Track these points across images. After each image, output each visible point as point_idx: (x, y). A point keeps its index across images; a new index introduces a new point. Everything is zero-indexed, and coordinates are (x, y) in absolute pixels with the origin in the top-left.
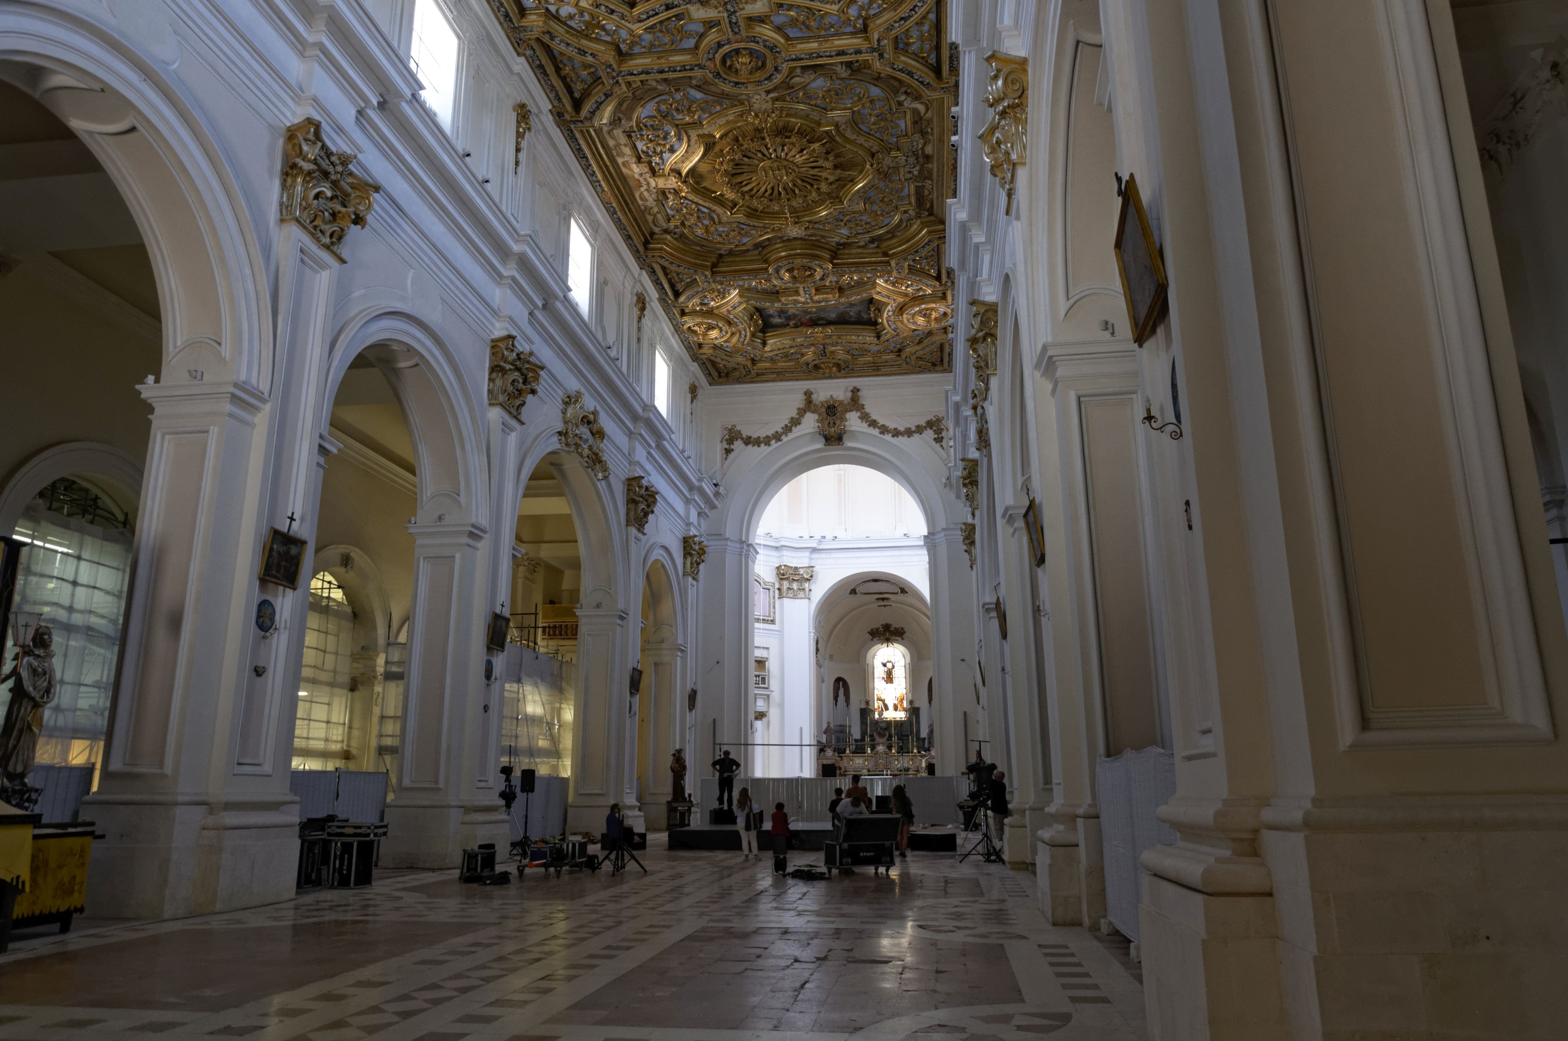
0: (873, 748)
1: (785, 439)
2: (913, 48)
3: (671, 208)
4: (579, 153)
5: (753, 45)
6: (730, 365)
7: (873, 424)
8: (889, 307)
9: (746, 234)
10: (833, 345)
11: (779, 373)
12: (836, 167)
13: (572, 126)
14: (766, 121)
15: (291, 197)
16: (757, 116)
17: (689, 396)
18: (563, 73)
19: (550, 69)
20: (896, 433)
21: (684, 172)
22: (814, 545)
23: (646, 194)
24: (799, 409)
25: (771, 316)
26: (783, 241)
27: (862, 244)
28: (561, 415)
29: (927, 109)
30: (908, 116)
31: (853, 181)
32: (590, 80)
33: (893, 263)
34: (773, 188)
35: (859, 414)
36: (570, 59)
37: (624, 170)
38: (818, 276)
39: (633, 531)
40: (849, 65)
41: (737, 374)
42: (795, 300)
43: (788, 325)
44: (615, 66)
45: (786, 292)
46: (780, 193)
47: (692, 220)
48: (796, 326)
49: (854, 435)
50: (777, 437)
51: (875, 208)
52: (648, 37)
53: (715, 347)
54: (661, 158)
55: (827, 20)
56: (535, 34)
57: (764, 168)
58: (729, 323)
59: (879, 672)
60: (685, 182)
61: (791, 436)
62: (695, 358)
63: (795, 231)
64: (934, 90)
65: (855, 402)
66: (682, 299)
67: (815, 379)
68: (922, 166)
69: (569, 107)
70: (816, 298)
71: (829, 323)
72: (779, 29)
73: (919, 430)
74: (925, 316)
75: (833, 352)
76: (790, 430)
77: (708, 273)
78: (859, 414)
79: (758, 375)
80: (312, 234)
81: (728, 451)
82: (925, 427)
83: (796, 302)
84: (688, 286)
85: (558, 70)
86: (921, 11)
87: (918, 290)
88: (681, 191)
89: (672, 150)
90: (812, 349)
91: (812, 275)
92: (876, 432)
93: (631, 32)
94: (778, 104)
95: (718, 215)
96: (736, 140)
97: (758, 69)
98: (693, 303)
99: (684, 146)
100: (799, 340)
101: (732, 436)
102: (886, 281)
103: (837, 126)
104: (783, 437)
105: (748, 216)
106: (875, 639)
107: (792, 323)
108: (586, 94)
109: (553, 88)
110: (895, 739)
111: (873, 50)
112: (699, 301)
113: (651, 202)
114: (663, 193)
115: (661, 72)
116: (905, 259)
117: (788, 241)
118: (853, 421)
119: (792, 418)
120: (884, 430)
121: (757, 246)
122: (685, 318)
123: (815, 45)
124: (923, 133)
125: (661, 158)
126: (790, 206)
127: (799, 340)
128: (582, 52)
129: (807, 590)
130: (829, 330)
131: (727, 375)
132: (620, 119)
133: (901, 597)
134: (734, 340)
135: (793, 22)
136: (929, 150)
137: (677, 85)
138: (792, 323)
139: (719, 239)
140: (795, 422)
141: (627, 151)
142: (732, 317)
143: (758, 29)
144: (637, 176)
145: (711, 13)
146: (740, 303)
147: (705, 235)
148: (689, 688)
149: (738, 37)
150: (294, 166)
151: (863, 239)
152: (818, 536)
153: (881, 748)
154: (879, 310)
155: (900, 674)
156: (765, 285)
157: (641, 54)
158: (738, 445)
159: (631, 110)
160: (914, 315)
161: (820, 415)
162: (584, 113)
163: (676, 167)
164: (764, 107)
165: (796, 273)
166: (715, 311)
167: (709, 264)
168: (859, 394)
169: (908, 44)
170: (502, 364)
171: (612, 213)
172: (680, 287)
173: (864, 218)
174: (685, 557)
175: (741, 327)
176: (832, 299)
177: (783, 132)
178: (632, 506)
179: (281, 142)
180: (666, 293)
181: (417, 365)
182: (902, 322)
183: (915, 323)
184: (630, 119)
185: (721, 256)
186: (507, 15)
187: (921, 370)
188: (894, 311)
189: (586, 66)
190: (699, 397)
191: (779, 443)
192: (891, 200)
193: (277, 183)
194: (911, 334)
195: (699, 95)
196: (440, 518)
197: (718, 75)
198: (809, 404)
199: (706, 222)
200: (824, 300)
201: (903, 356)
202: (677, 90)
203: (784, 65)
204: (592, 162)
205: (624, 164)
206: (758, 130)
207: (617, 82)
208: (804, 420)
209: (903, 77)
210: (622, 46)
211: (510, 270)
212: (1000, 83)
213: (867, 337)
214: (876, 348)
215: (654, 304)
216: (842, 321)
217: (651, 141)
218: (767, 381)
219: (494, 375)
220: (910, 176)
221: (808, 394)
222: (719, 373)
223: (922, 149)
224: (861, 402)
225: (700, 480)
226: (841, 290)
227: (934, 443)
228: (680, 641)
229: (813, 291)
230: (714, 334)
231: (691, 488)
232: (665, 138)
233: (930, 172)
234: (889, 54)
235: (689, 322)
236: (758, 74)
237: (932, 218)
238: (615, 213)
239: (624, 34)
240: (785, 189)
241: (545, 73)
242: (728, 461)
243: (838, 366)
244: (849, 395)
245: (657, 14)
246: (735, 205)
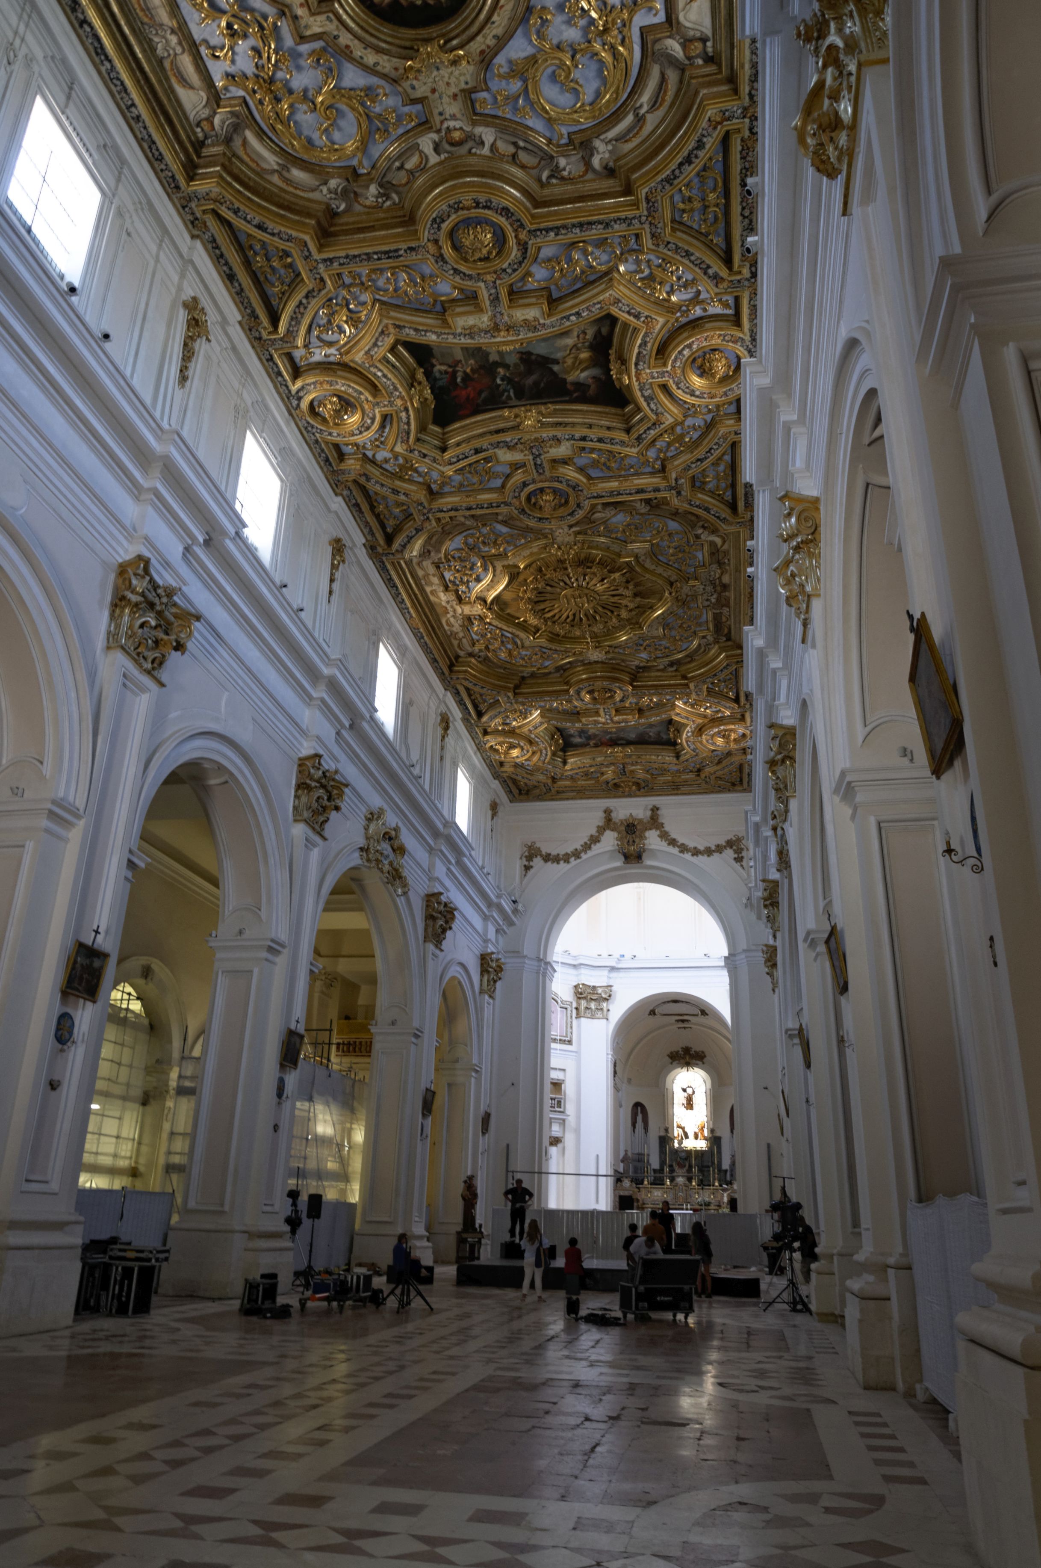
0: (672, 1180)
2: (710, 486)
3: (476, 633)
4: (390, 583)
5: (556, 485)
6: (530, 783)
7: (673, 842)
8: (688, 728)
9: (548, 658)
10: (632, 764)
11: (579, 791)
12: (636, 595)
13: (384, 558)
14: (568, 553)
15: (118, 626)
16: (559, 548)
17: (490, 813)
18: (377, 511)
19: (365, 507)
20: (696, 852)
21: (489, 600)
22: (613, 964)
23: (452, 620)
24: (598, 827)
25: (572, 736)
26: (584, 665)
27: (661, 667)
28: (363, 831)
29: (724, 542)
30: (706, 548)
31: (652, 608)
32: (402, 517)
33: (692, 685)
34: (574, 615)
35: (658, 832)
36: (384, 498)
37: (432, 598)
38: (618, 698)
39: (431, 947)
40: (648, 501)
41: (537, 792)
43: (588, 744)
44: (426, 504)
45: (587, 712)
46: (581, 619)
47: (496, 644)
48: (596, 746)
49: (654, 853)
50: (577, 854)
51: (674, 633)
52: (458, 478)
53: (516, 765)
54: (468, 587)
55: (627, 462)
56: (352, 476)
57: (566, 596)
58: (531, 742)
59: (679, 1098)
60: (490, 609)
61: (590, 854)
62: (496, 776)
63: (595, 655)
64: (731, 524)
65: (654, 821)
66: (485, 719)
67: (615, 797)
68: (719, 594)
69: (382, 542)
70: (616, 719)
71: (629, 743)
72: (581, 470)
73: (719, 849)
74: (723, 737)
75: (632, 772)
76: (590, 848)
77: (510, 694)
78: (658, 832)
79: (558, 792)
80: (135, 661)
81: (527, 868)
82: (725, 847)
83: (597, 722)
84: (491, 706)
85: (372, 508)
86: (716, 454)
87: (717, 712)
88: (486, 617)
89: (478, 580)
90: (612, 768)
91: (612, 697)
92: (675, 851)
93: (442, 474)
94: (580, 538)
95: (521, 640)
96: (540, 570)
97: (561, 505)
98: (496, 723)
99: (490, 576)
100: (599, 759)
101: (532, 853)
102: (685, 703)
103: (637, 557)
104: (582, 855)
105: (551, 640)
106: (675, 1063)
107: (592, 743)
108: (398, 529)
109: (367, 524)
110: (695, 1170)
111: (671, 488)
112: (501, 721)
113: (457, 627)
114: (469, 619)
115: (469, 509)
116: (704, 682)
117: (589, 665)
118: (652, 839)
119: (592, 836)
120: (684, 848)
121: (559, 669)
122: (488, 737)
123: (615, 484)
124: (720, 564)
125: (468, 587)
126: (591, 632)
127: (599, 759)
128: (396, 492)
130: (629, 750)
131: (528, 792)
132: (429, 552)
133: (701, 1019)
134: (535, 758)
135: (595, 464)
136: (726, 579)
137: (483, 520)
138: (592, 743)
139: (521, 662)
140: (595, 840)
141: (435, 580)
143: (561, 470)
144: (444, 604)
145: (517, 456)
146: (541, 723)
147: (508, 659)
148: (482, 1109)
149: (542, 477)
150: (123, 598)
152: (616, 955)
153: (680, 1180)
155: (701, 1101)
156: (566, 706)
157: (450, 493)
158: (537, 862)
159: (440, 543)
160: (713, 736)
161: (619, 833)
162: (396, 545)
163: (482, 595)
164: (567, 539)
165: (596, 694)
166: (517, 731)
167: (511, 686)
168: (659, 812)
169: (704, 483)
170: (308, 781)
171: (419, 637)
172: (483, 707)
173: (663, 642)
174: (482, 974)
175: (542, 746)
176: (632, 720)
177: (584, 562)
178: (430, 923)
179: (112, 576)
180: (469, 713)
181: (226, 782)
182: (701, 742)
183: (714, 744)
184: (439, 551)
185: (523, 678)
186: (327, 460)
187: (721, 790)
188: (693, 732)
189: (399, 504)
190: (500, 814)
191: (579, 861)
192: (689, 627)
193: (106, 614)
194: (710, 754)
195: (504, 529)
196: (241, 932)
198: (609, 822)
199: (510, 646)
201: (703, 776)
202: (484, 525)
203: (586, 502)
204: (402, 591)
205: (432, 592)
206: (561, 561)
207: (428, 518)
208: (603, 838)
209: (700, 512)
210: (433, 486)
211: (320, 692)
212: (793, 520)
213: (666, 757)
214: (675, 768)
215: (458, 725)
216: (642, 741)
217: (458, 571)
218: (567, 799)
219: (300, 792)
220: (707, 603)
221: (608, 812)
222: (520, 790)
223: (720, 578)
224: (661, 820)
225: (499, 896)
226: (640, 711)
227: (734, 862)
228: (475, 1061)
229: (614, 712)
230: (515, 753)
231: (490, 904)
232: (472, 569)
233: (728, 600)
234: (686, 491)
235: (491, 741)
236: (562, 509)
237: (730, 643)
238: (423, 637)
239: (435, 475)
240: (586, 615)
241: (360, 511)
243: (638, 784)
244: (649, 813)
245: (466, 457)
246: (538, 630)
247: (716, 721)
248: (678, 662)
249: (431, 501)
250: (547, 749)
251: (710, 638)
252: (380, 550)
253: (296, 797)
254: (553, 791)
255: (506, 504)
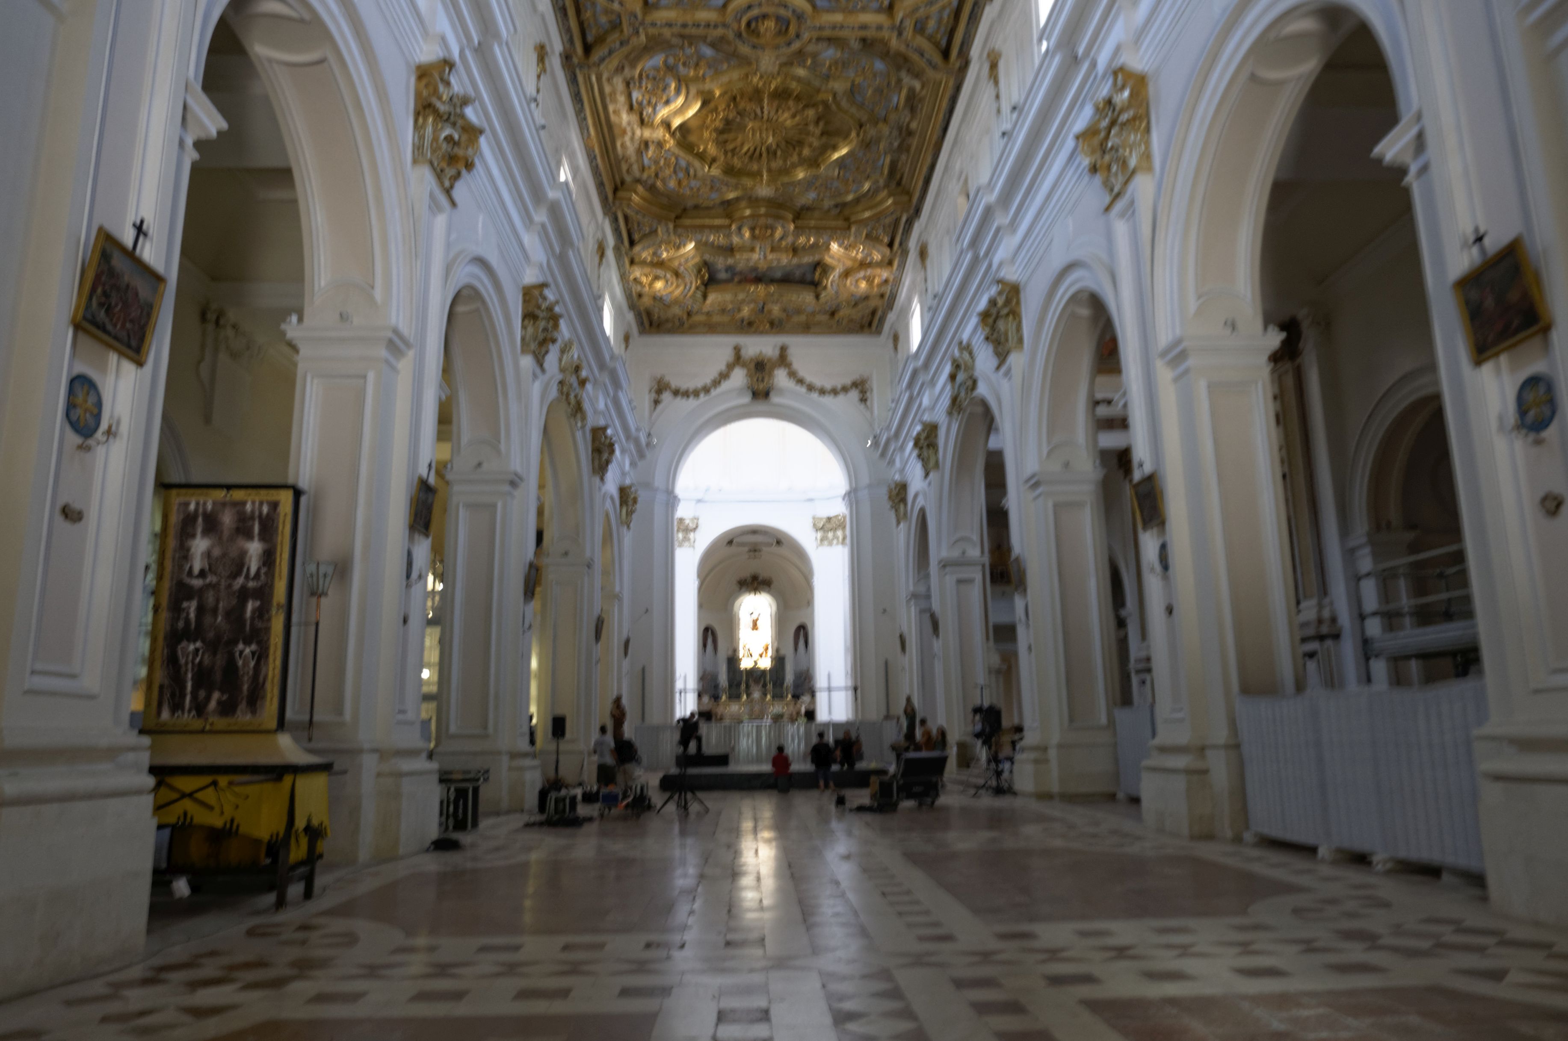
0: (748, 695)
1: (714, 392)
4: (577, 97)
5: (782, 12)
7: (801, 381)
12: (822, 134)
15: (422, 138)
16: (761, 77)
19: (571, 12)
20: (822, 392)
23: (628, 143)
29: (923, 87)
30: (904, 93)
31: (835, 148)
33: (853, 229)
37: (613, 118)
39: (597, 480)
40: (864, 40)
41: (670, 325)
45: (742, 249)
46: (761, 155)
47: (668, 172)
48: (740, 282)
49: (781, 392)
50: (706, 390)
53: (655, 298)
58: (677, 274)
60: (673, 134)
61: (719, 390)
62: (632, 306)
63: (764, 191)
65: (783, 359)
66: (637, 249)
69: (579, 50)
71: (772, 281)
77: (671, 226)
81: (657, 402)
84: (645, 236)
85: (578, 12)
89: (667, 102)
90: (752, 306)
91: (772, 235)
92: (803, 390)
95: (695, 171)
96: (734, 99)
98: (646, 255)
101: (660, 388)
103: (835, 96)
106: (743, 589)
108: (601, 40)
109: (569, 30)
110: (770, 686)
113: (631, 150)
114: (646, 144)
115: (684, 26)
117: (753, 201)
118: (781, 377)
120: (811, 388)
129: (692, 540)
130: (772, 289)
131: (659, 326)
132: (623, 68)
133: (775, 549)
136: (914, 125)
137: (691, 40)
138: (736, 279)
140: (724, 376)
141: (622, 99)
148: (624, 636)
151: (827, 203)
153: (756, 695)
158: (666, 396)
161: (749, 370)
162: (595, 57)
171: (591, 158)
172: (636, 237)
174: (621, 505)
176: (785, 259)
177: (781, 95)
179: (413, 79)
180: (622, 242)
185: (685, 210)
188: (840, 277)
189: (607, 11)
190: (630, 347)
191: (707, 398)
195: (708, 52)
196: (479, 465)
197: (739, 35)
198: (738, 359)
201: (837, 317)
209: (915, 57)
211: (541, 216)
213: (805, 298)
215: (610, 254)
216: (787, 280)
219: (526, 322)
221: (737, 350)
222: (651, 324)
225: (638, 430)
226: (795, 250)
228: (617, 589)
229: (769, 250)
230: (659, 285)
233: (909, 146)
234: (908, 33)
235: (637, 272)
242: (655, 414)
243: (772, 324)
244: (777, 352)
247: (863, 265)
248: (844, 205)
249: (645, 14)
250: (693, 282)
251: (881, 182)
252: (575, 60)
253: (524, 327)
254: (686, 325)
255: (725, 25)
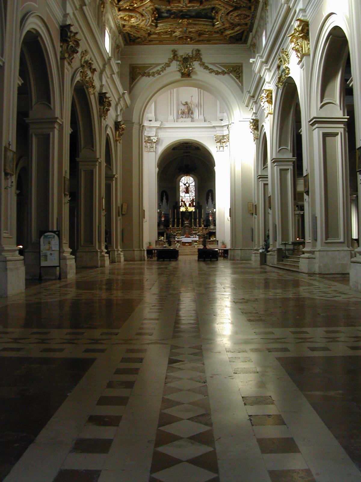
6: (137, 36)
8: (223, 12)
25: (163, 12)
42: (177, 6)
43: (170, 17)
48: (174, 18)
53: (132, 27)
58: (142, 15)
59: (182, 187)
61: (165, 72)
66: (121, 3)
70: (189, 5)
71: (191, 17)
78: (199, 62)
90: (180, 30)
107: (172, 16)
112: (128, 4)
122: (121, 13)
142: (144, 12)
154: (217, 12)
155: (192, 188)
166: (137, 10)
175: (147, 17)
200: (193, 7)
208: (171, 64)
216: (198, 16)
221: (174, 52)
222: (130, 40)
230: (133, 20)
250: (149, 19)
